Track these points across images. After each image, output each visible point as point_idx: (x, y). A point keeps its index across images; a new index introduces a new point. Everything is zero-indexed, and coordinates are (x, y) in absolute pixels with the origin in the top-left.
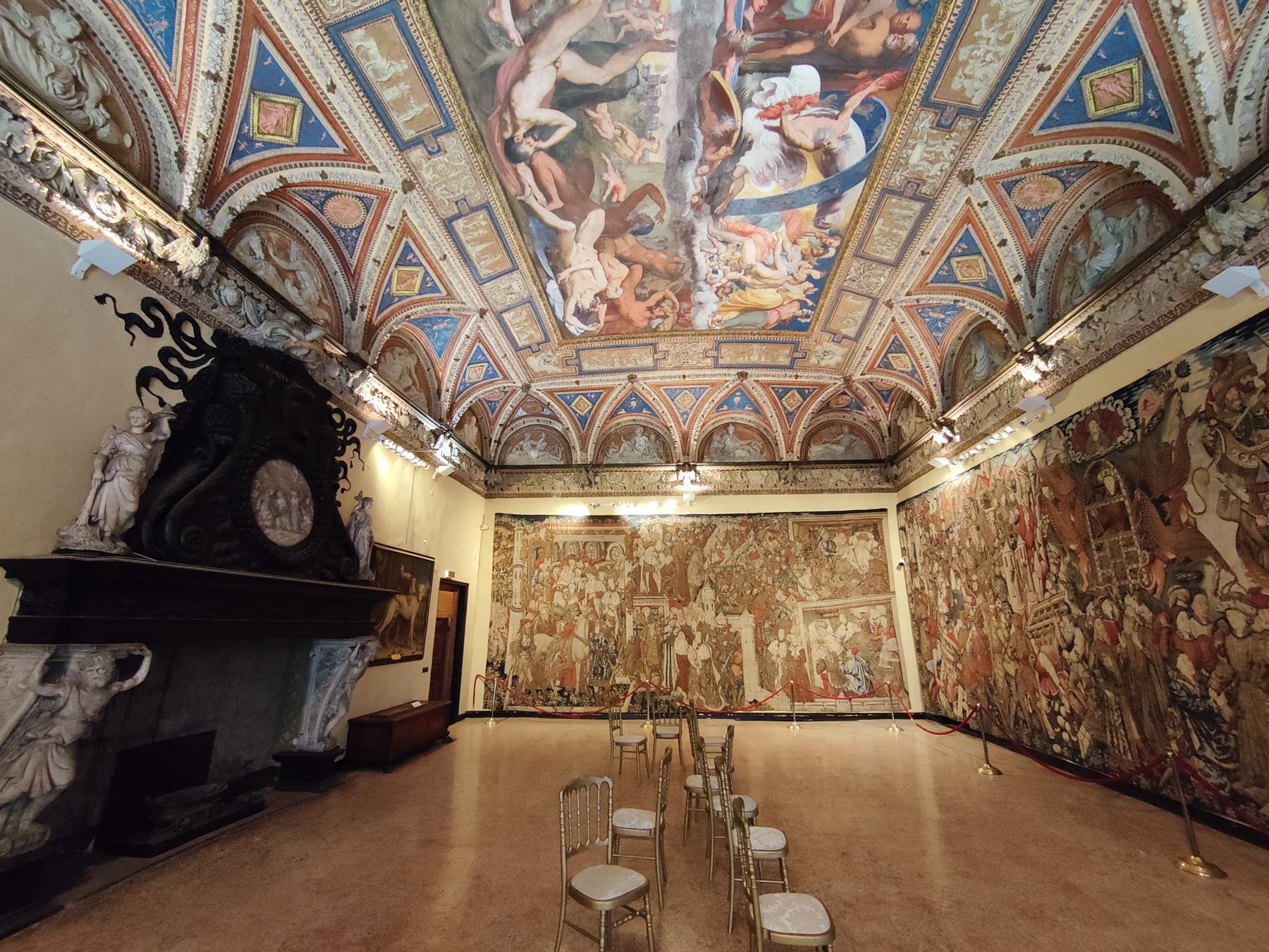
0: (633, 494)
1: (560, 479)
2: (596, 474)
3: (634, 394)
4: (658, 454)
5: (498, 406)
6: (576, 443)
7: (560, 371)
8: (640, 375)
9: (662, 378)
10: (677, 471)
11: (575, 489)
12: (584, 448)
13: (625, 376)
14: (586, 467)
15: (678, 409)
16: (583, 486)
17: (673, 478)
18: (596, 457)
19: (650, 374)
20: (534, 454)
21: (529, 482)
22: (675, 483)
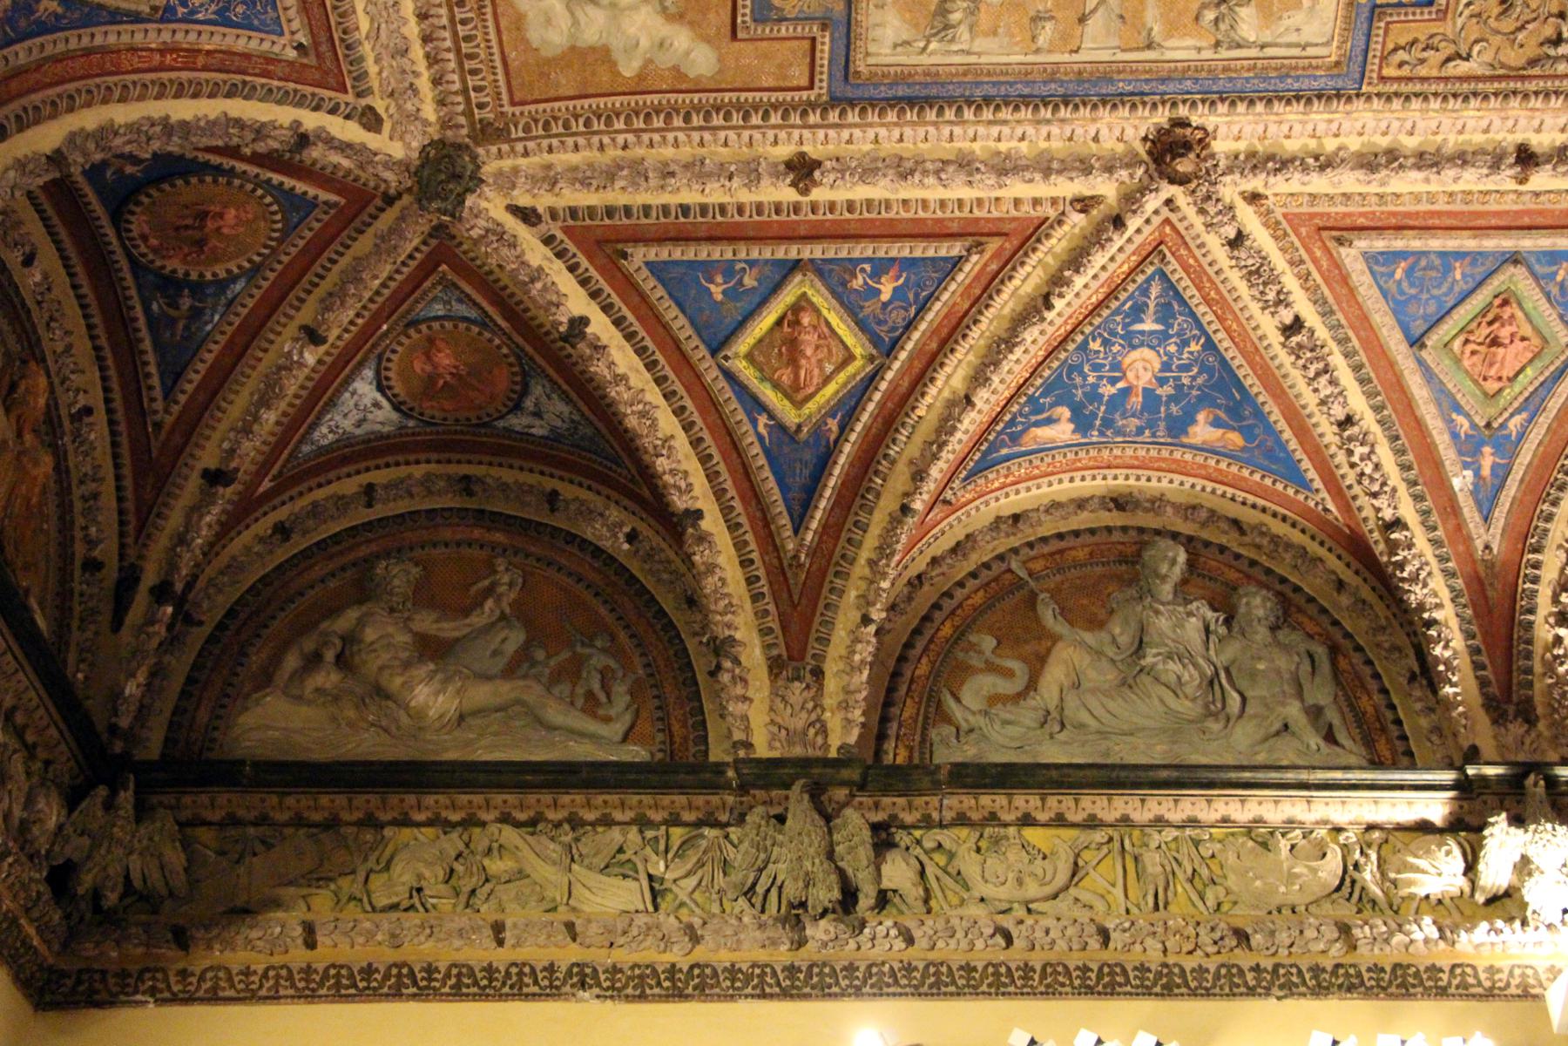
0: (1165, 983)
1: (618, 865)
2: (883, 838)
3: (1162, 291)
4: (1314, 713)
5: (219, 327)
6: (744, 627)
7: (702, 60)
8: (1231, 130)
9: (1369, 162)
10: (1465, 827)
11: (747, 941)
12: (795, 659)
13: (1125, 129)
14: (815, 779)
15: (1449, 405)
16: (795, 916)
17: (1439, 872)
18: (878, 731)
19: (1294, 129)
20: (431, 698)
21: (391, 886)
22: (1456, 913)
